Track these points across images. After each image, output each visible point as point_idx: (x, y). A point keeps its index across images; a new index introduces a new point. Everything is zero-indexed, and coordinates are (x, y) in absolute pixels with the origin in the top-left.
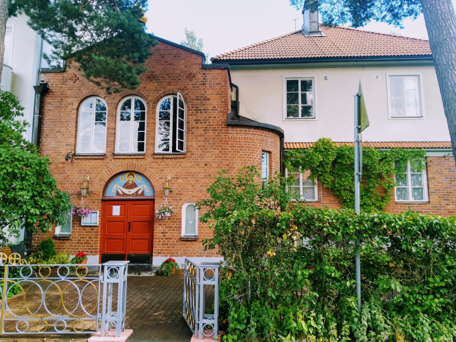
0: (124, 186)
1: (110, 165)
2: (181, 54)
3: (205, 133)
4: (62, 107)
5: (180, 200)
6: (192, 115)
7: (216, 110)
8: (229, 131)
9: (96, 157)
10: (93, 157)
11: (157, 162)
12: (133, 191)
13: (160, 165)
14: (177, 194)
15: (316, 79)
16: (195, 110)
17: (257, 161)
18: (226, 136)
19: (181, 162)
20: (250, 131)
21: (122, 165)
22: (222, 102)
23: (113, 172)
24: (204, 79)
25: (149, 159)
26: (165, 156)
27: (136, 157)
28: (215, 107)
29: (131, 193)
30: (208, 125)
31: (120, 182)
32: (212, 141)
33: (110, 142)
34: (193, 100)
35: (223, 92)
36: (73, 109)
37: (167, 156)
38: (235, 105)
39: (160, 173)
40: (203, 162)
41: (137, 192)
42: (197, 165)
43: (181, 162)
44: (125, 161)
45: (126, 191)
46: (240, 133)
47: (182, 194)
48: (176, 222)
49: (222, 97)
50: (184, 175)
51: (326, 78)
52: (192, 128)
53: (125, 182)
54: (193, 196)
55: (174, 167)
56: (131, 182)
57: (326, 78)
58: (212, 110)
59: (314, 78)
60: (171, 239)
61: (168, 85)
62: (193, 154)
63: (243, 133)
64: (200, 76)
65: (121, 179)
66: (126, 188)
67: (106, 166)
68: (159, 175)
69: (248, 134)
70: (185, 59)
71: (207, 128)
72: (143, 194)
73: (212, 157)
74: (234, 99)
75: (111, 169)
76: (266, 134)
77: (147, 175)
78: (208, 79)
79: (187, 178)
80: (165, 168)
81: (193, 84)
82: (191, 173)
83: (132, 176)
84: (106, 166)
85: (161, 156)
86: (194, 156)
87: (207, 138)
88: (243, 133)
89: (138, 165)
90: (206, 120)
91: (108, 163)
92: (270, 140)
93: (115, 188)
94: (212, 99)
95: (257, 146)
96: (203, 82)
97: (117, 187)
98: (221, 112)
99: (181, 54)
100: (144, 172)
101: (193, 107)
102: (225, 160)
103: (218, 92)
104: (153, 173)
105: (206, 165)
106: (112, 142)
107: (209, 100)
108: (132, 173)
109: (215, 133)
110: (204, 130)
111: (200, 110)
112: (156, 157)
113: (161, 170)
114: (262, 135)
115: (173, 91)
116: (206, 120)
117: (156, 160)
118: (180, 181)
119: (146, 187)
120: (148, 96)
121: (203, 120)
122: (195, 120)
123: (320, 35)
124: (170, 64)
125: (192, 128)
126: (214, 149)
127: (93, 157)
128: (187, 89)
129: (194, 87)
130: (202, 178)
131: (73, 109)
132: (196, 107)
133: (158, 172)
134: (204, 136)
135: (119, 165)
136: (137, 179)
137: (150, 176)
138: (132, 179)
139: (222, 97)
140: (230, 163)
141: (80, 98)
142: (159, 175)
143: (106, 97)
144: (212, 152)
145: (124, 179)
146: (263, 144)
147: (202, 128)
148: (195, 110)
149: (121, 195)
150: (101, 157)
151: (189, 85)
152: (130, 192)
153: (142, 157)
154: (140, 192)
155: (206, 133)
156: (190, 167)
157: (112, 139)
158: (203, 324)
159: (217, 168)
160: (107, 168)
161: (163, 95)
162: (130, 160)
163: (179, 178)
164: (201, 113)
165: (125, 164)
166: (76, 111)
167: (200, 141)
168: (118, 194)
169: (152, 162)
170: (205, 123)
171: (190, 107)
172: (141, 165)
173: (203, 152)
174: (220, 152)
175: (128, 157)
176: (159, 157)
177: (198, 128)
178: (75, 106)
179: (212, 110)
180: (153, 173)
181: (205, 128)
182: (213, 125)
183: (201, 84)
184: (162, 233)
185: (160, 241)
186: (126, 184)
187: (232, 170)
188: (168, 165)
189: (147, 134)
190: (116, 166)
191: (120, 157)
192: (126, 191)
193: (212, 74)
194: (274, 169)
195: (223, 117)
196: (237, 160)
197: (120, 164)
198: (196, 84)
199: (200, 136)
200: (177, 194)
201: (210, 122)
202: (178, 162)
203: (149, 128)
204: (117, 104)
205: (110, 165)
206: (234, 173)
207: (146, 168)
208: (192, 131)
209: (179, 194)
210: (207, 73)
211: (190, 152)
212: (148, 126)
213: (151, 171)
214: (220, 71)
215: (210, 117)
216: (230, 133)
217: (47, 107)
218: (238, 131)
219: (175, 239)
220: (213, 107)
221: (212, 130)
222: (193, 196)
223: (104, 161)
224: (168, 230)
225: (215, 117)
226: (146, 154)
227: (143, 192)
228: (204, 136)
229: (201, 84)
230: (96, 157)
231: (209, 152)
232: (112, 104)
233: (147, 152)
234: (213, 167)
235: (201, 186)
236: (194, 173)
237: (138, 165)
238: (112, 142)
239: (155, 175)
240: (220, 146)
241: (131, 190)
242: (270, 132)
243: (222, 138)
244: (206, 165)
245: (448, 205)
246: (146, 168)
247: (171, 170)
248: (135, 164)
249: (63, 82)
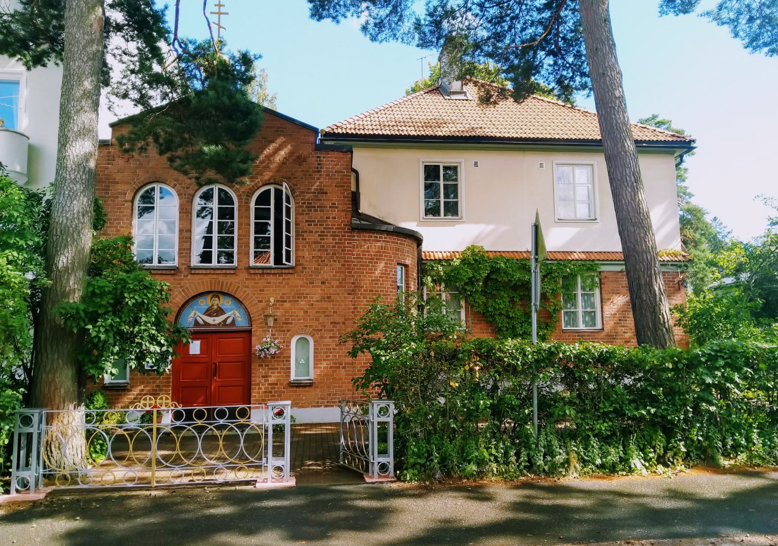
0: (206, 312)
1: (186, 283)
2: (286, 128)
3: (321, 239)
4: (109, 197)
5: (288, 331)
6: (303, 214)
7: (337, 207)
8: (354, 236)
9: (164, 272)
10: (160, 272)
11: (253, 279)
12: (219, 319)
13: (258, 283)
14: (283, 323)
15: (463, 164)
17: (391, 278)
18: (351, 243)
19: (289, 279)
20: (382, 238)
21: (203, 282)
22: (344, 197)
23: (189, 292)
24: (318, 164)
25: (243, 275)
26: (265, 271)
27: (224, 271)
28: (335, 204)
29: (216, 322)
30: (324, 228)
31: (199, 307)
32: (331, 250)
33: (184, 250)
35: (344, 183)
36: (127, 201)
37: (269, 271)
38: (355, 198)
39: (258, 294)
40: (319, 279)
41: (225, 321)
42: (311, 283)
43: (289, 279)
44: (207, 278)
45: (210, 320)
46: (370, 240)
47: (291, 323)
48: (283, 361)
49: (344, 190)
50: (294, 297)
51: (476, 164)
52: (302, 232)
53: (206, 307)
54: (306, 326)
55: (279, 286)
56: (216, 307)
57: (476, 164)
58: (330, 207)
59: (460, 163)
60: (276, 384)
62: (306, 268)
63: (373, 240)
64: (312, 160)
65: (202, 302)
66: (210, 315)
67: (179, 284)
68: (257, 298)
69: (380, 241)
71: (324, 232)
73: (332, 272)
74: (353, 189)
75: (187, 288)
76: (402, 241)
77: (241, 297)
78: (324, 164)
79: (298, 301)
80: (265, 287)
81: (303, 171)
82: (303, 294)
83: (217, 299)
84: (179, 284)
85: (260, 271)
86: (307, 270)
87: (324, 246)
88: (373, 240)
89: (227, 283)
90: (323, 221)
91: (181, 280)
92: (407, 249)
93: (192, 315)
94: (330, 193)
95: (390, 257)
96: (318, 168)
97: (195, 314)
98: (343, 211)
99: (286, 128)
100: (235, 293)
102: (350, 276)
103: (338, 183)
104: (248, 294)
105: (323, 283)
106: (187, 249)
107: (326, 193)
108: (217, 294)
109: (336, 239)
110: (319, 236)
111: (315, 207)
112: (252, 271)
113: (260, 291)
114: (397, 243)
115: (275, 179)
116: (323, 221)
117: (253, 276)
118: (287, 305)
121: (318, 221)
122: (307, 221)
123: (465, 98)
125: (302, 232)
126: (335, 261)
127: (160, 272)
128: (295, 178)
129: (305, 175)
130: (317, 301)
131: (127, 201)
132: (308, 203)
133: (256, 293)
134: (320, 243)
135: (198, 283)
136: (225, 303)
137: (243, 300)
138: (216, 302)
139: (344, 190)
140: (356, 280)
141: (137, 185)
142: (257, 298)
143: (176, 185)
144: (331, 265)
145: (205, 303)
146: (397, 254)
147: (317, 232)
148: (307, 207)
149: (202, 325)
150: (172, 272)
151: (298, 171)
152: (214, 321)
153: (232, 272)
154: (229, 321)
155: (323, 239)
156: (301, 286)
157: (186, 245)
158: (379, 463)
159: (337, 287)
160: (181, 287)
161: (261, 184)
162: (215, 276)
163: (286, 301)
164: (315, 211)
165: (207, 282)
166: (130, 204)
167: (314, 250)
168: (196, 323)
169: (247, 279)
170: (320, 225)
171: (299, 203)
172: (231, 284)
173: (319, 265)
174: (342, 265)
175: (212, 272)
176: (257, 272)
177: (311, 232)
178: (129, 197)
179: (330, 207)
180: (248, 294)
181: (322, 232)
182: (333, 228)
183: (314, 172)
184: (263, 377)
185: (260, 388)
186: (208, 310)
187: (359, 290)
188: (270, 283)
189: (239, 239)
190: (195, 285)
191: (200, 272)
192: (210, 320)
193: (330, 157)
195: (346, 218)
196: (366, 276)
197: (200, 281)
198: (307, 171)
199: (315, 243)
200: (283, 323)
201: (328, 225)
202: (284, 279)
203: (241, 231)
204: (193, 196)
205: (186, 283)
206: (361, 294)
207: (238, 287)
208: (303, 236)
209: (287, 323)
210: (322, 156)
211: (301, 264)
212: (239, 229)
213: (245, 291)
214: (341, 155)
215: (328, 218)
216: (356, 240)
218: (366, 237)
219: (281, 384)
220: (332, 204)
221: (331, 236)
222: (306, 326)
223: (176, 277)
224: (272, 373)
225: (334, 218)
226: (239, 267)
227: (233, 320)
228: (320, 243)
229: (314, 172)
230: (164, 272)
231: (327, 265)
232: (185, 195)
233: (238, 265)
234: (333, 287)
235: (317, 312)
236: (306, 294)
237: (227, 283)
238: (187, 249)
239: (252, 297)
240: (342, 258)
241: (216, 318)
242: (406, 238)
243: (344, 247)
244: (323, 283)
246: (238, 287)
247: (274, 290)
248: (223, 282)
249: (109, 160)
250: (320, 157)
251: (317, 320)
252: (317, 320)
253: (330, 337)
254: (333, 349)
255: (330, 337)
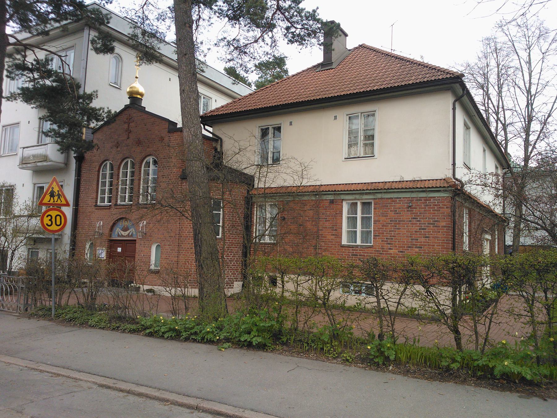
2: (156, 122)
5: (151, 240)
12: (126, 233)
14: (149, 236)
16: (163, 167)
24: (169, 141)
29: (125, 235)
34: (161, 159)
41: (129, 234)
45: (123, 233)
58: (173, 166)
61: (148, 148)
64: (166, 139)
70: (158, 125)
72: (132, 236)
99: (156, 122)
101: (162, 165)
119: (134, 231)
120: (136, 158)
121: (167, 175)
122: (162, 176)
124: (150, 131)
127: (104, 208)
150: (109, 208)
154: (130, 234)
162: (124, 209)
163: (150, 223)
168: (119, 236)
177: (164, 182)
192: (123, 233)
194: (227, 214)
217: (84, 171)
245: (390, 249)
250: (169, 136)
251: (163, 234)
252: (163, 234)
253: (168, 245)
254: (169, 252)
255: (168, 245)
